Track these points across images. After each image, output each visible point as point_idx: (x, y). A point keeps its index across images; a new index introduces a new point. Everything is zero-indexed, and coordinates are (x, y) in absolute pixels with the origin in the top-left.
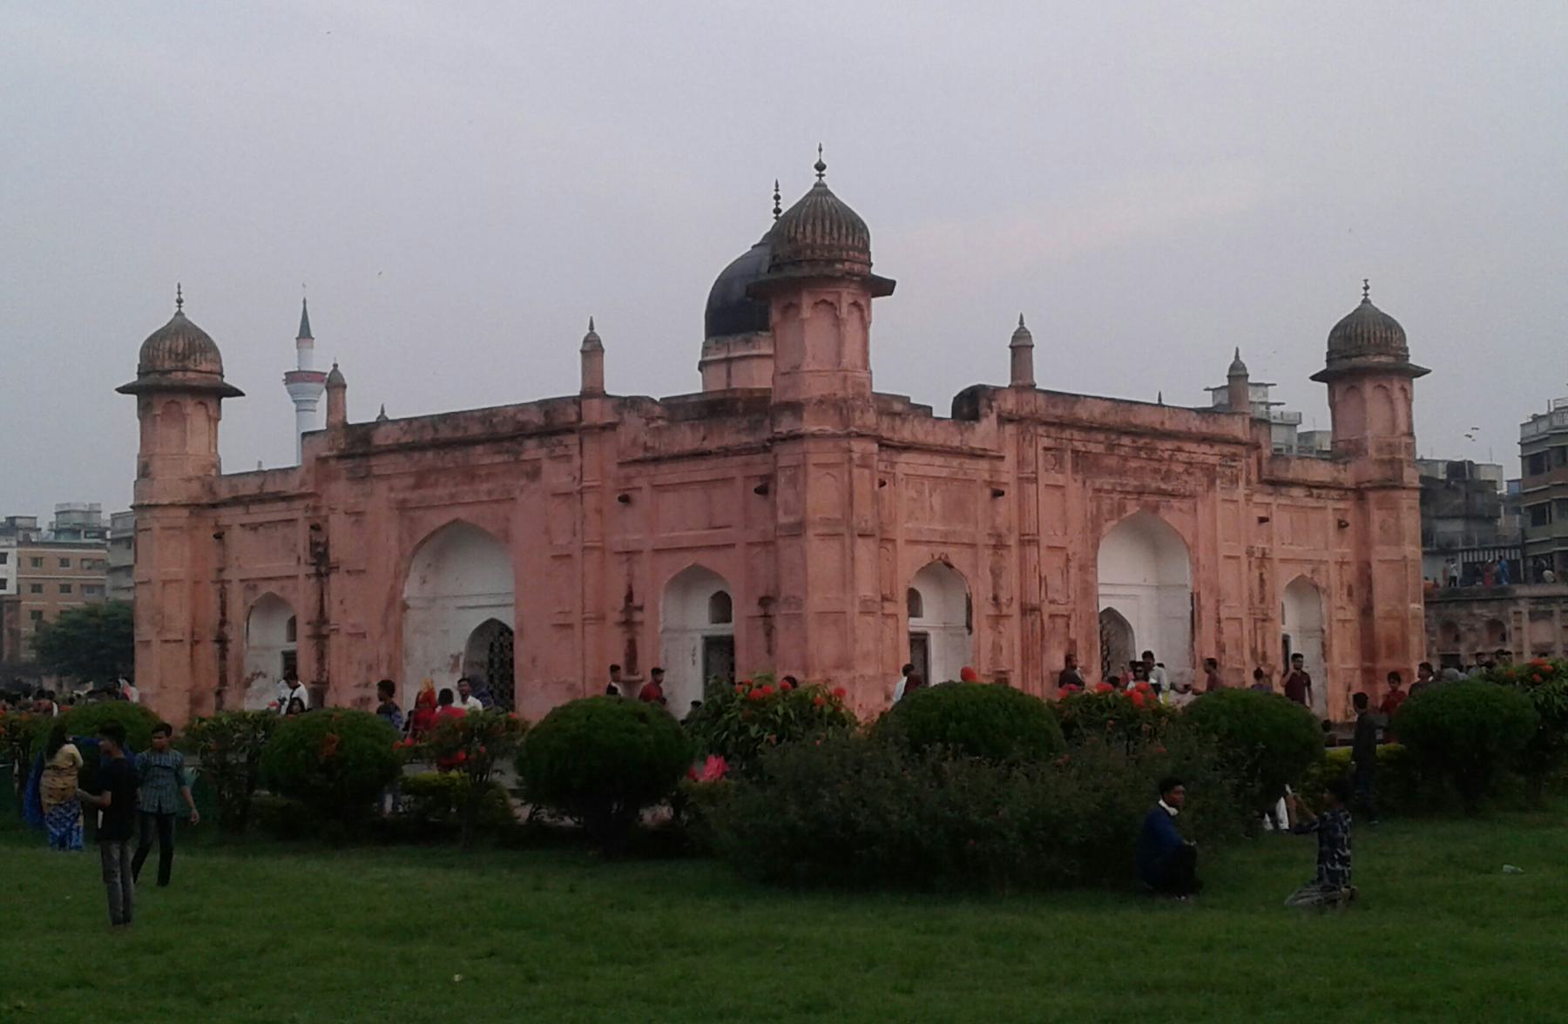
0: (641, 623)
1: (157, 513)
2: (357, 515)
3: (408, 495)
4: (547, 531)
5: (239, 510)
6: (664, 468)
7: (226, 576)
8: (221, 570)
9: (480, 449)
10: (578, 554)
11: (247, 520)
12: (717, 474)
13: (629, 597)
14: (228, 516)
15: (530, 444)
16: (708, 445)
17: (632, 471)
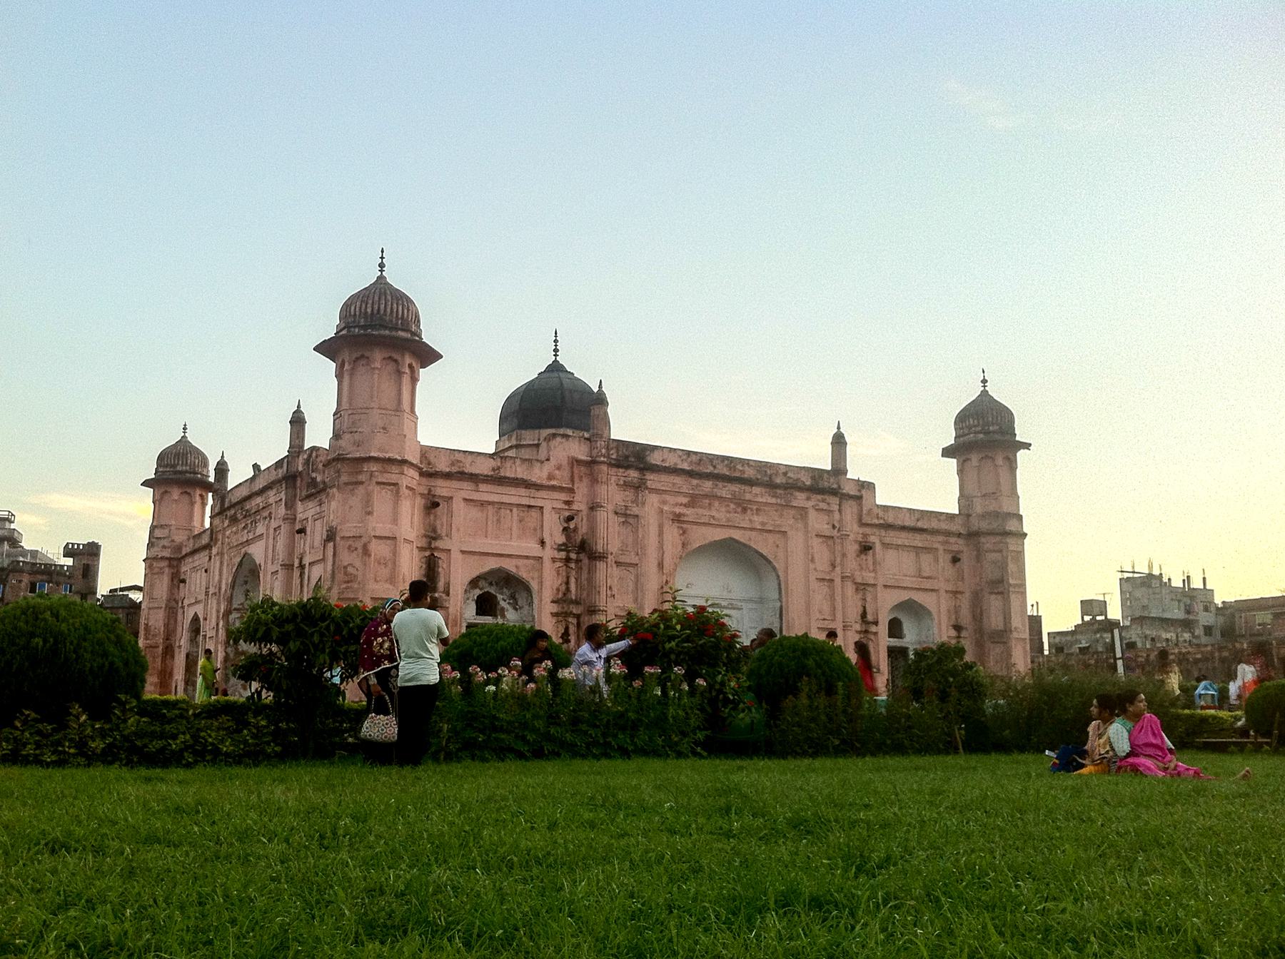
0: (876, 634)
2: (627, 517)
4: (812, 560)
5: (466, 485)
6: (892, 533)
7: (439, 544)
8: (435, 539)
9: (756, 490)
10: (838, 581)
11: (475, 496)
12: (926, 544)
13: (864, 615)
16: (920, 524)
17: (868, 530)
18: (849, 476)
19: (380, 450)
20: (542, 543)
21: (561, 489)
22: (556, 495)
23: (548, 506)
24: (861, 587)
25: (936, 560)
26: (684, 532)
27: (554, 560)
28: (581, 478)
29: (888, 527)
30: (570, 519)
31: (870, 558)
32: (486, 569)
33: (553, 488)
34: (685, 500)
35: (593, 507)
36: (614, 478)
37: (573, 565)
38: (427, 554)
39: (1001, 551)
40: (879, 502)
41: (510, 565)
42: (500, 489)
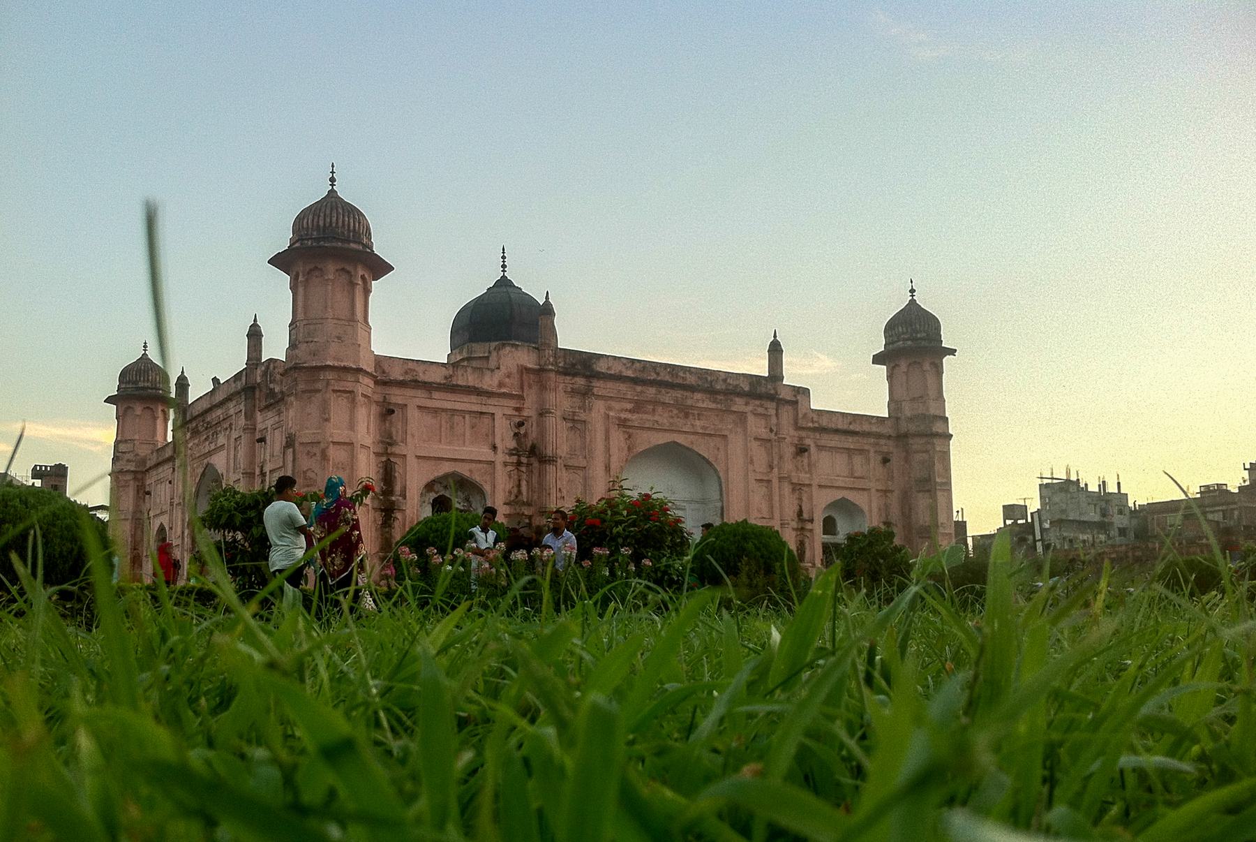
0: (811, 530)
2: (575, 423)
3: (629, 416)
4: (752, 462)
5: (419, 393)
6: (825, 436)
7: (396, 450)
8: (390, 444)
9: (698, 396)
10: (775, 482)
11: (429, 403)
12: (857, 446)
13: (800, 513)
16: (852, 427)
17: (803, 434)
18: (785, 382)
19: (334, 358)
20: (494, 448)
23: (499, 413)
24: (797, 487)
25: (868, 460)
27: (505, 464)
29: (823, 430)
30: (520, 424)
32: (441, 473)
34: (629, 406)
35: (543, 413)
36: (561, 386)
37: (524, 469)
38: (384, 459)
39: (927, 451)
41: (463, 470)
42: (450, 396)
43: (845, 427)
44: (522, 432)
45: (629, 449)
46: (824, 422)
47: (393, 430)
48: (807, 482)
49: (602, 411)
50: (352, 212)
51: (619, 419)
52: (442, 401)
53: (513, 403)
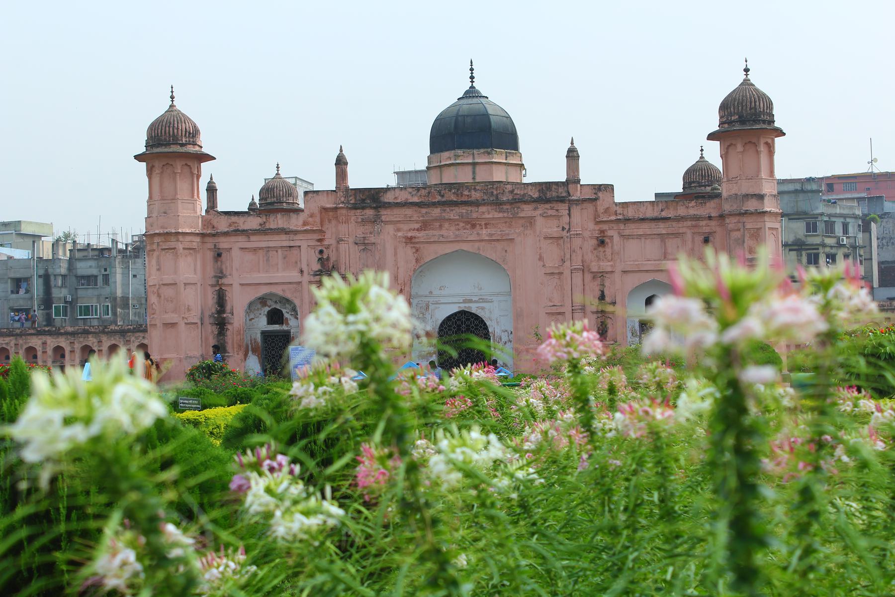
1: (181, 238)
6: (632, 226)
8: (221, 278)
9: (483, 209)
10: (567, 273)
11: (248, 245)
12: (670, 231)
14: (224, 243)
15: (526, 207)
16: (664, 214)
17: (605, 227)
19: (162, 227)
20: (302, 272)
21: (313, 231)
22: (310, 236)
23: (304, 245)
24: (600, 276)
26: (417, 250)
28: (330, 221)
29: (627, 220)
31: (608, 250)
33: (306, 231)
35: (339, 241)
36: (353, 218)
38: (217, 288)
40: (617, 200)
41: (278, 290)
43: (656, 214)
44: (325, 257)
45: (417, 260)
46: (630, 213)
47: (224, 267)
48: (609, 269)
49: (392, 233)
50: (184, 119)
51: (406, 238)
52: (257, 242)
53: (316, 236)
